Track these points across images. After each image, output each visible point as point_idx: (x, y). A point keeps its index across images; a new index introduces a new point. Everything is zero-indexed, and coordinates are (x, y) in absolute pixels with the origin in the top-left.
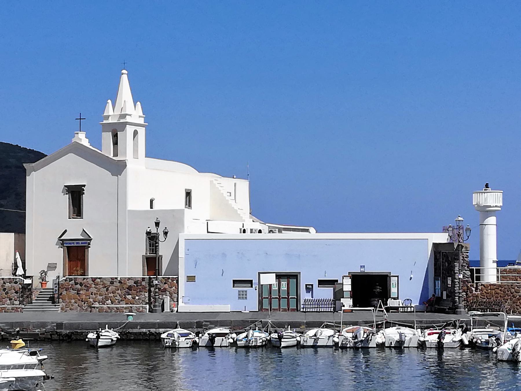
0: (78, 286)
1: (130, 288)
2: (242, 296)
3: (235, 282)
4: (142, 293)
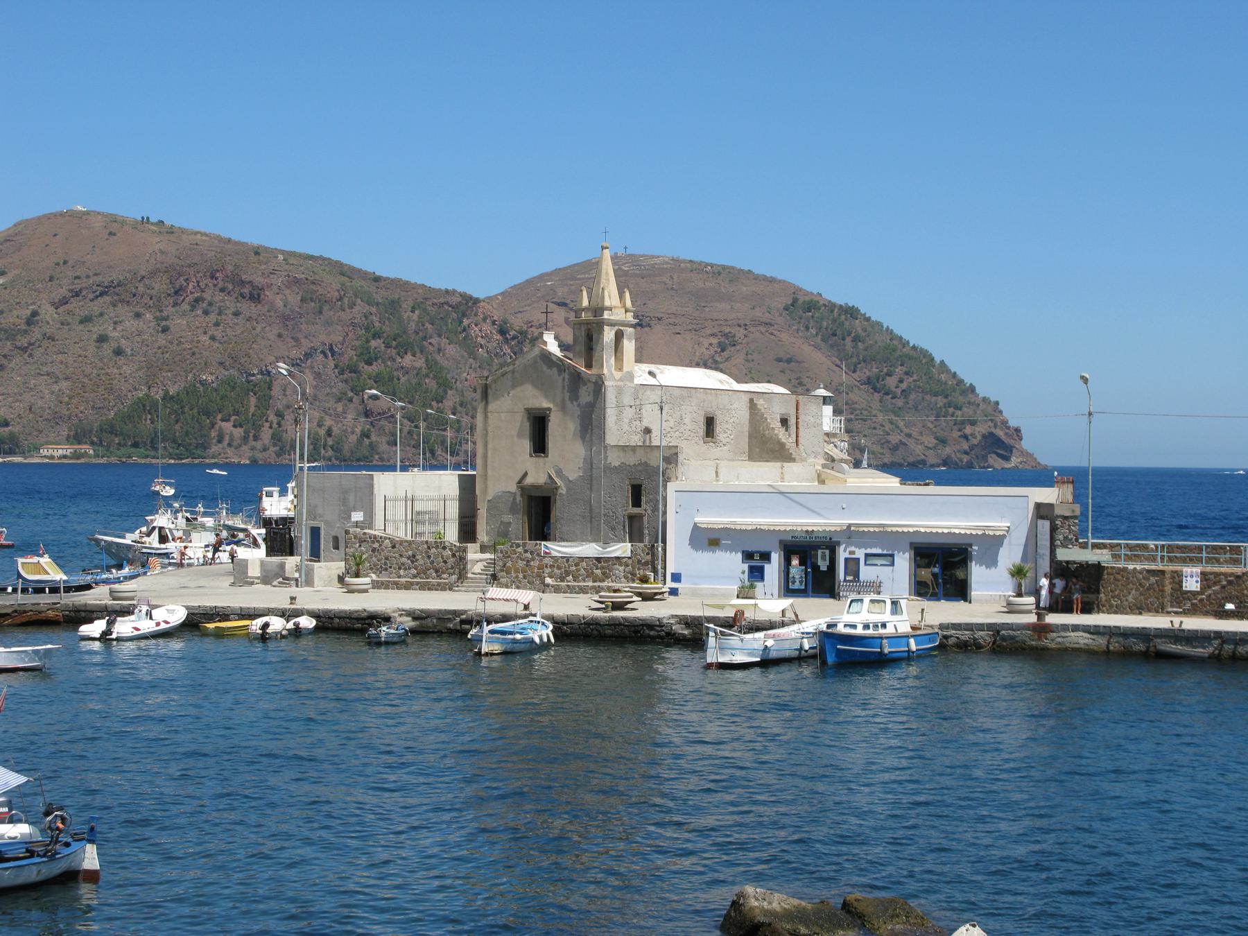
0: (528, 555)
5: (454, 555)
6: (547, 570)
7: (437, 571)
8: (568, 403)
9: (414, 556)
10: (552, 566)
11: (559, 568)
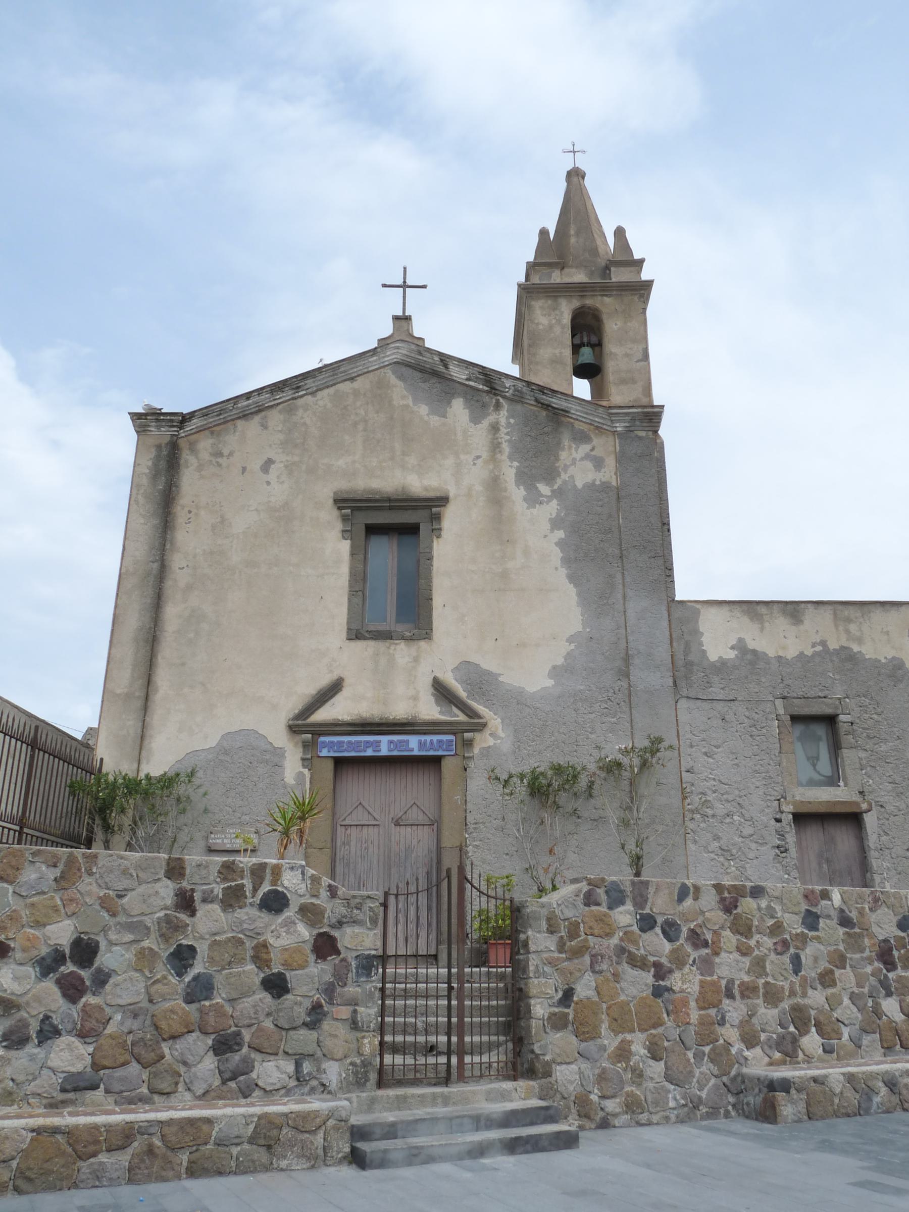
5: (325, 946)
6: (735, 1010)
7: (224, 1045)
8: (517, 493)
9: (84, 951)
10: (748, 991)
11: (772, 996)
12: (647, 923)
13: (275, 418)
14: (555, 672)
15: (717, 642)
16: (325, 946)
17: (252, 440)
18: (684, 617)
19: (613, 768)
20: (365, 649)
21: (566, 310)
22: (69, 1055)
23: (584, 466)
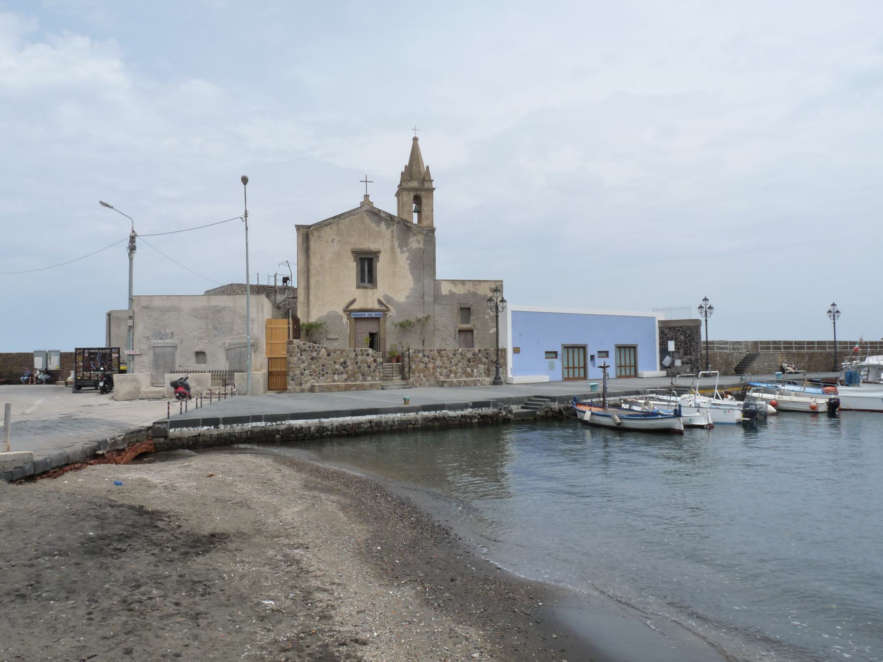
1: (469, 361)
2: (552, 367)
3: (546, 352)
4: (480, 365)
5: (375, 361)
6: (439, 370)
7: (363, 375)
8: (398, 250)
9: (345, 362)
10: (441, 367)
11: (446, 368)
12: (424, 356)
13: (334, 226)
14: (407, 297)
15: (445, 290)
16: (375, 361)
17: (329, 233)
18: (437, 284)
19: (419, 321)
20: (361, 291)
21: (412, 195)
22: (345, 376)
23: (415, 243)
